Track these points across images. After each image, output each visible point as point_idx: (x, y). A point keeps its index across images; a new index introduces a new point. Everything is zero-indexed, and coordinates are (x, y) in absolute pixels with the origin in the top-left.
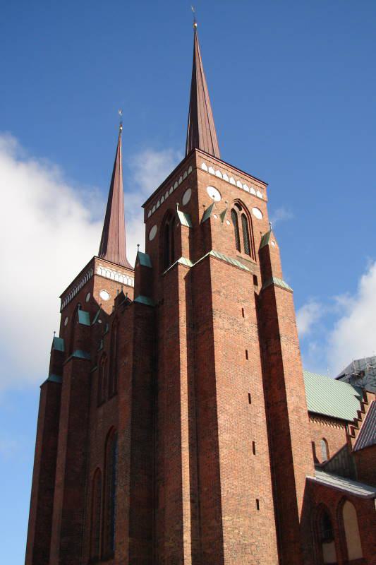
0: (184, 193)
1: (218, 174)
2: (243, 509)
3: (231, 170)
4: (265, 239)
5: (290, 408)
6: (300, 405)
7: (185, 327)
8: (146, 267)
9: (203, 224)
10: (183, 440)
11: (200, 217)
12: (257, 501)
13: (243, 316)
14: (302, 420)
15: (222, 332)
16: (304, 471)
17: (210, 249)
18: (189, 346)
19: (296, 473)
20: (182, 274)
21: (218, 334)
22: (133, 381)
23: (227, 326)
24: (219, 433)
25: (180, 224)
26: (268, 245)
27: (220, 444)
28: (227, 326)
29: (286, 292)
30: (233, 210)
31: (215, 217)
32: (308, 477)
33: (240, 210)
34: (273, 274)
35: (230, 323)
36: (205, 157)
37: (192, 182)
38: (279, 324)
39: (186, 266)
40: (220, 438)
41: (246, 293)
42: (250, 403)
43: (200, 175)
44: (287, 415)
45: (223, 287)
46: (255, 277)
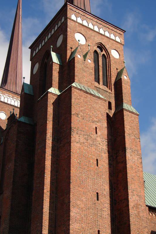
1: (85, 23)
3: (96, 20)
4: (119, 74)
5: (131, 204)
6: (139, 202)
7: (51, 141)
8: (28, 94)
9: (69, 61)
10: (44, 227)
11: (68, 57)
14: (141, 215)
15: (78, 145)
17: (74, 81)
18: (53, 155)
20: (51, 100)
22: (13, 181)
23: (82, 140)
24: (71, 223)
25: (53, 62)
26: (121, 79)
28: (82, 140)
29: (133, 115)
30: (96, 52)
31: (79, 57)
33: (102, 51)
34: (124, 101)
35: (85, 138)
36: (75, 9)
37: (63, 30)
38: (126, 140)
39: (54, 94)
40: (71, 227)
41: (100, 115)
42: (98, 200)
43: (69, 23)
44: (128, 210)
45: (81, 111)
46: (110, 103)
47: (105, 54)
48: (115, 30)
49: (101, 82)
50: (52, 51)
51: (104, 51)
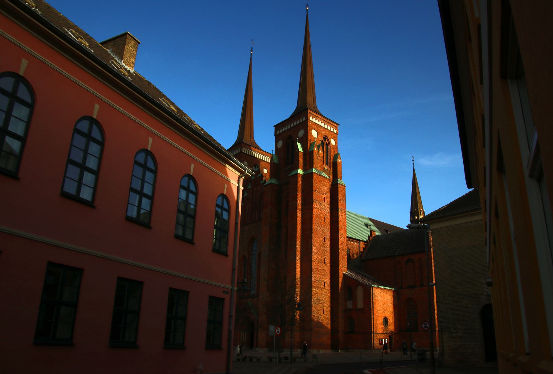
0: (299, 132)
2: (319, 286)
5: (340, 242)
8: (276, 163)
9: (309, 152)
12: (325, 283)
13: (325, 202)
14: (344, 248)
16: (343, 270)
19: (340, 271)
20: (300, 179)
21: (315, 211)
23: (318, 207)
26: (337, 162)
27: (313, 260)
28: (318, 207)
30: (322, 141)
32: (344, 273)
33: (325, 141)
36: (312, 113)
39: (300, 174)
42: (325, 241)
47: (327, 142)
48: (334, 124)
49: (325, 164)
50: (298, 142)
51: (327, 140)
